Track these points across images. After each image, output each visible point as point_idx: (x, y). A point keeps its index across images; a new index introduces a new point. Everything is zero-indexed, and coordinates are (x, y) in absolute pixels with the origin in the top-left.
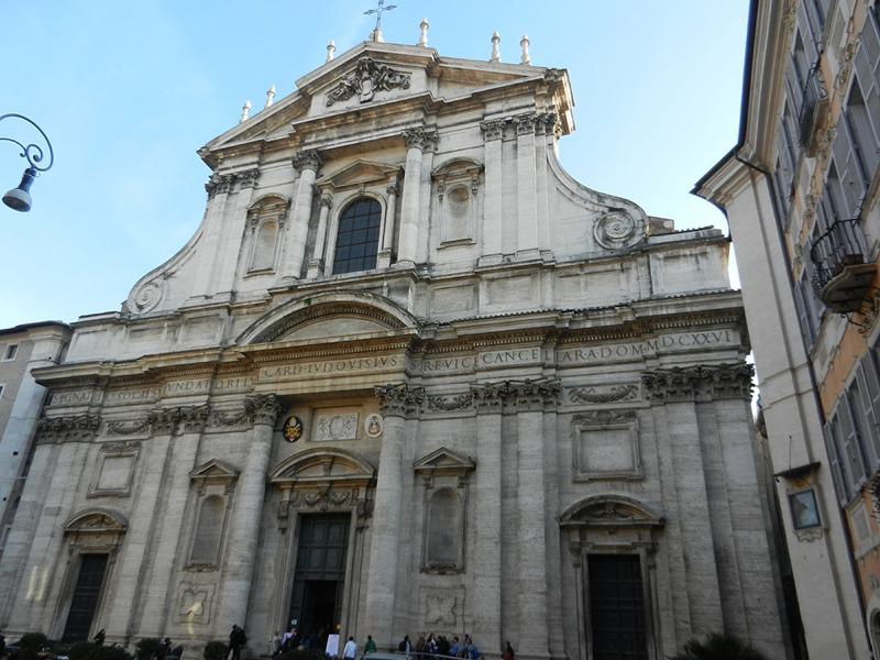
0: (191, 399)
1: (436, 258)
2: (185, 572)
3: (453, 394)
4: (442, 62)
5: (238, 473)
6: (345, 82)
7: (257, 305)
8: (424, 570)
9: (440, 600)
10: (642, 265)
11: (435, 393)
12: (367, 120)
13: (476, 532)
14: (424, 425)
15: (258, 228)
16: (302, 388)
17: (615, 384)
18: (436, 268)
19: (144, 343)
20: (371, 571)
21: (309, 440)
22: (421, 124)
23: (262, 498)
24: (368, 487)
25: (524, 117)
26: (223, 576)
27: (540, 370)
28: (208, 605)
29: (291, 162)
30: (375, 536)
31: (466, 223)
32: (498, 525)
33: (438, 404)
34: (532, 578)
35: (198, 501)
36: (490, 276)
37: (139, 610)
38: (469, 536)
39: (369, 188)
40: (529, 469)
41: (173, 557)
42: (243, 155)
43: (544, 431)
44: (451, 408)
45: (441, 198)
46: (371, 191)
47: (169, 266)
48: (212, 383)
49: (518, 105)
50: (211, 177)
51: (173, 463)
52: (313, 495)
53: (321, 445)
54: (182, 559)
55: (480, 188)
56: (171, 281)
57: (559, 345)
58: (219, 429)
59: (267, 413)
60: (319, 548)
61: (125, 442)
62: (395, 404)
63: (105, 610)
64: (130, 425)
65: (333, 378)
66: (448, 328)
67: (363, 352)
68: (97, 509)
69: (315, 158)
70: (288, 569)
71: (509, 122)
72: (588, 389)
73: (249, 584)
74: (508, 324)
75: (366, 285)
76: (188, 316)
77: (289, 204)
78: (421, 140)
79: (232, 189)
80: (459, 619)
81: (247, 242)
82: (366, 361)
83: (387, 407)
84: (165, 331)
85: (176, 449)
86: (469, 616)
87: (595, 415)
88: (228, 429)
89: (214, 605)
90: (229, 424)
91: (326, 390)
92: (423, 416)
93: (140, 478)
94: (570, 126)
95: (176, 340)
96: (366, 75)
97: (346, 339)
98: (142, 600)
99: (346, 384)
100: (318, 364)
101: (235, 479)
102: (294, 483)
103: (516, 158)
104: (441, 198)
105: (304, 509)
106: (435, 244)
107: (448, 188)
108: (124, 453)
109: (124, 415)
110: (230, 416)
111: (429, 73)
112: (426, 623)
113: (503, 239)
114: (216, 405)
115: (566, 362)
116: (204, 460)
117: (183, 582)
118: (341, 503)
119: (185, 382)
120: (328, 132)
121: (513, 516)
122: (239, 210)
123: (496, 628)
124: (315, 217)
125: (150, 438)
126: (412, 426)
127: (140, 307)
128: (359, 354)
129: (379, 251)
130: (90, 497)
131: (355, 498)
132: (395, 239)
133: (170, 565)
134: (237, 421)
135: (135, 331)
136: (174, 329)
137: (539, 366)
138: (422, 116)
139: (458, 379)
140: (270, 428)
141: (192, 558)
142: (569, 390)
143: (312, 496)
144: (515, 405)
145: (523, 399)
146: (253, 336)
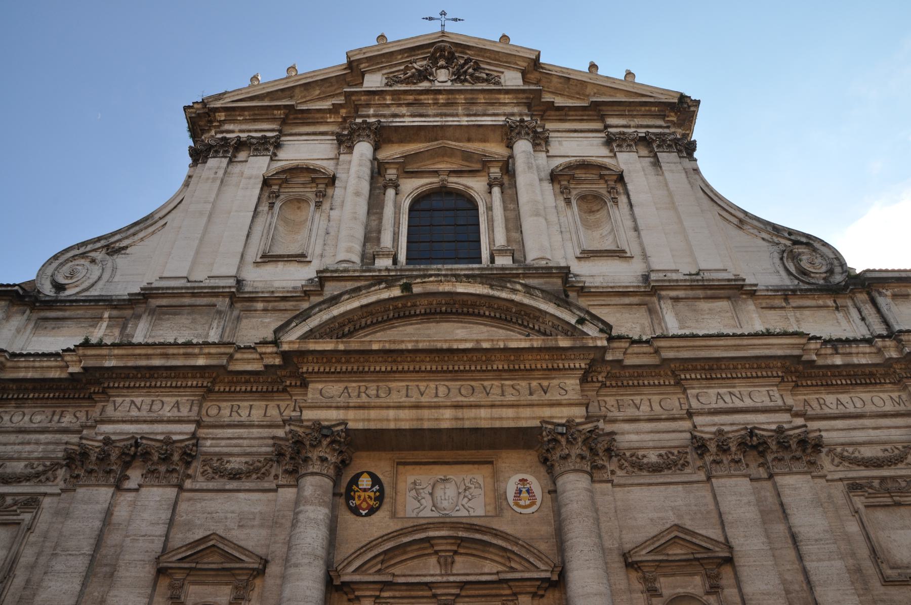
1: (577, 268)
3: (655, 448)
4: (543, 68)
5: (265, 562)
6: (415, 65)
7: (284, 299)
10: (864, 302)
11: (626, 445)
14: (620, 493)
15: (278, 204)
16: (396, 420)
17: (885, 443)
19: (62, 339)
21: (394, 515)
22: (529, 119)
27: (786, 417)
33: (638, 465)
36: (673, 294)
40: (820, 560)
42: (255, 120)
44: (656, 469)
48: (200, 407)
56: (120, 260)
58: (211, 485)
62: (579, 451)
65: (457, 406)
67: (509, 371)
71: (642, 139)
72: (851, 449)
74: (737, 347)
76: (154, 302)
77: (332, 180)
81: (261, 221)
82: (513, 386)
85: (121, 513)
87: (876, 483)
91: (445, 425)
96: (442, 63)
97: (485, 345)
99: (483, 418)
100: (422, 385)
101: (261, 572)
104: (568, 202)
107: (574, 192)
110: (235, 463)
113: (673, 256)
114: (209, 443)
115: (810, 412)
119: (148, 400)
126: (604, 494)
127: (59, 287)
128: (499, 374)
134: (248, 474)
135: (46, 319)
140: (328, 483)
144: (761, 465)
145: (779, 455)
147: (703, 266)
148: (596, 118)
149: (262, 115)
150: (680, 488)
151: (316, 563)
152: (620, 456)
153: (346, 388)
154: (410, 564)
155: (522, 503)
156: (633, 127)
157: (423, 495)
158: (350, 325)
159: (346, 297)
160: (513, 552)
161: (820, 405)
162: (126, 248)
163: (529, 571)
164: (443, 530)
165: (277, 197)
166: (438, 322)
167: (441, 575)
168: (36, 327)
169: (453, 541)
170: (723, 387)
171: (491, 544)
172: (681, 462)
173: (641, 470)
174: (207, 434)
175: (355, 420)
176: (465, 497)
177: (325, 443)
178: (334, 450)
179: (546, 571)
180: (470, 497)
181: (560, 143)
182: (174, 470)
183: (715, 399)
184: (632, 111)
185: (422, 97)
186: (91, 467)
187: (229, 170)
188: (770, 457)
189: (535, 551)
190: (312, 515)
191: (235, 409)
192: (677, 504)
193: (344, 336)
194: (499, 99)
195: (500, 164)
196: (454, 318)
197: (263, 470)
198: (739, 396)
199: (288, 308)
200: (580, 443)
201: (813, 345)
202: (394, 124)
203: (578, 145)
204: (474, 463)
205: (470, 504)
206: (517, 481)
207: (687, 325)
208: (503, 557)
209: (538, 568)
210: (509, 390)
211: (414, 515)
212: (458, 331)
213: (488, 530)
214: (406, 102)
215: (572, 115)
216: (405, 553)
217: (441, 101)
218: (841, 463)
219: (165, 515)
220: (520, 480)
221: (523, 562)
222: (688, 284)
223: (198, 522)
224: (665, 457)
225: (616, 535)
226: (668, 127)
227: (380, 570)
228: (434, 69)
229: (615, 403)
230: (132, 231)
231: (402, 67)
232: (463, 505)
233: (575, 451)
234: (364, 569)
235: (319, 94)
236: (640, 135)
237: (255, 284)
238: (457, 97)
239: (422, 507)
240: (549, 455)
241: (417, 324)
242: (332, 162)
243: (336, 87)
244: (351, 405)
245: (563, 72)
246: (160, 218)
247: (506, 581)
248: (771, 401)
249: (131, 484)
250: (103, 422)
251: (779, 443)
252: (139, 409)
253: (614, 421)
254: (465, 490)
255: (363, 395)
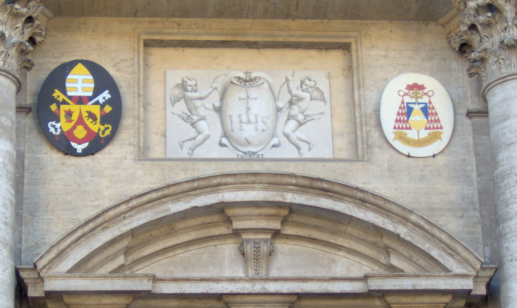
154: (182, 254)
155: (412, 134)
157: (202, 112)
160: (397, 237)
164: (253, 189)
167: (252, 280)
169: (273, 211)
171: (351, 220)
176: (290, 117)
178: (16, 16)
179: (464, 276)
180: (301, 117)
189: (443, 237)
205: (301, 133)
206: (403, 87)
208: (374, 245)
209: (447, 270)
211: (184, 154)
213: (346, 191)
216: (172, 232)
220: (410, 87)
221: (416, 257)
227: (121, 267)
232: (286, 135)
234: (90, 265)
239: (200, 138)
240: (475, 39)
247: (383, 294)
254: (291, 103)
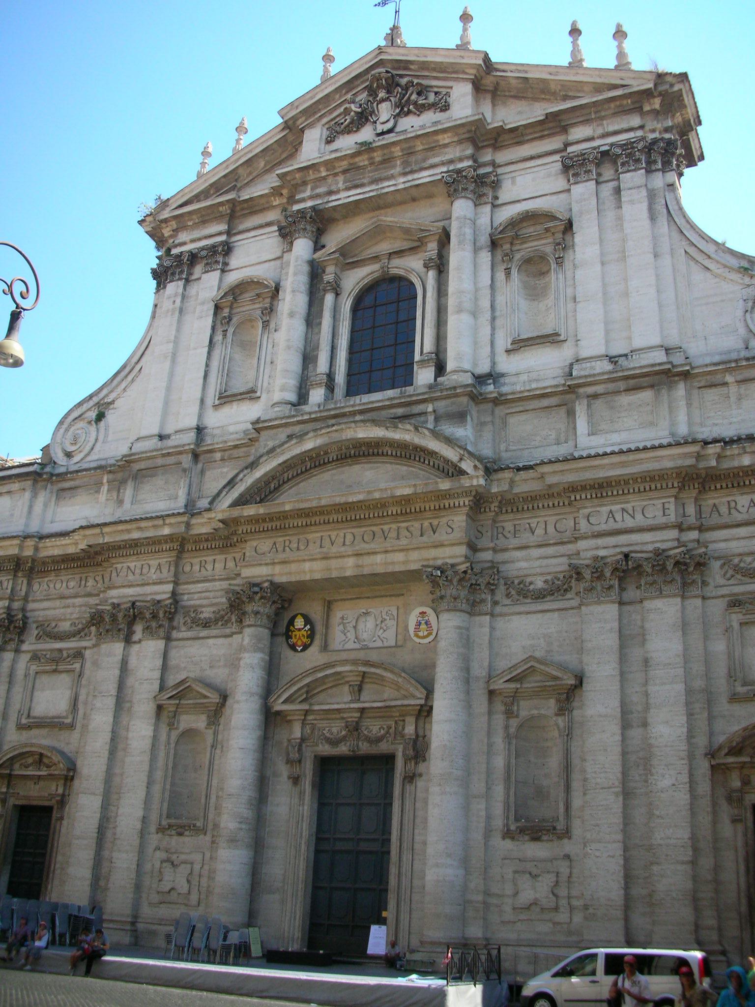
0: (148, 589)
1: (506, 364)
2: (160, 835)
4: (497, 70)
6: (353, 107)
7: (236, 447)
8: (508, 834)
9: (534, 877)
11: (515, 573)
12: (387, 161)
13: (585, 780)
14: (500, 623)
15: (231, 330)
18: (507, 380)
19: (77, 507)
20: (432, 838)
21: (325, 648)
23: (259, 733)
24: (418, 716)
25: (628, 146)
26: (213, 842)
27: (674, 534)
28: (195, 882)
29: (275, 228)
30: (434, 789)
31: (547, 310)
32: (618, 769)
34: (672, 841)
35: (169, 736)
36: (590, 390)
37: (102, 883)
38: (576, 785)
39: (396, 262)
40: (663, 684)
41: (140, 813)
43: (684, 626)
44: (540, 596)
45: (508, 272)
46: (398, 267)
47: (105, 392)
48: (177, 566)
49: (616, 127)
50: (158, 257)
51: (130, 681)
52: (336, 728)
53: (344, 656)
54: (154, 817)
55: (569, 256)
56: (111, 417)
57: (703, 490)
58: (189, 634)
59: (261, 610)
60: (349, 804)
61: (60, 650)
62: (454, 592)
63: (56, 882)
64: (65, 626)
66: (531, 473)
68: (32, 745)
69: (313, 220)
70: (305, 833)
72: (749, 559)
73: (252, 853)
74: (623, 464)
75: (400, 411)
78: (472, 187)
79: (190, 274)
80: (563, 902)
81: (216, 353)
83: (442, 597)
84: (105, 488)
85: (133, 662)
86: (577, 898)
88: (204, 633)
89: (204, 881)
90: (205, 626)
92: (498, 609)
93: (86, 703)
94: (696, 154)
95: (120, 502)
96: (382, 94)
98: (104, 871)
99: (377, 563)
100: (333, 534)
102: (307, 712)
103: (620, 207)
104: (508, 272)
105: (325, 749)
106: (503, 342)
107: (518, 256)
108: (61, 668)
109: (57, 612)
111: (478, 87)
112: (514, 909)
114: (186, 597)
116: (172, 680)
117: (158, 848)
118: (379, 740)
119: (139, 564)
120: (330, 180)
121: (641, 754)
122: (203, 303)
123: (620, 914)
124: (314, 309)
125: (94, 646)
127: (69, 455)
129: (417, 357)
130: (20, 727)
131: (399, 734)
132: (440, 338)
133: (139, 826)
135: (63, 490)
136: (118, 486)
137: (674, 527)
138: (469, 151)
139: (550, 550)
140: (266, 633)
141: (168, 817)
142: (719, 563)
143: (335, 730)
146: (235, 494)
147: (638, 343)
148: (558, 130)
149: (208, 215)
150: (556, 614)
151: (252, 699)
152: (509, 583)
153: (275, 543)
155: (421, 634)
156: (598, 138)
158: (275, 481)
159: (264, 458)
161: (729, 509)
162: (113, 402)
163: (405, 697)
165: (228, 322)
166: (351, 465)
168: (58, 498)
170: (616, 504)
172: (565, 587)
173: (525, 597)
174: (184, 590)
175: (281, 574)
177: (257, 597)
181: (514, 183)
182: (160, 626)
183: (605, 518)
184: (600, 111)
185: (357, 160)
186: (107, 627)
187: (186, 293)
188: (643, 582)
190: (248, 661)
191: (203, 563)
192: (549, 631)
193: (270, 492)
194: (438, 141)
195: (437, 237)
196: (363, 460)
197: (226, 618)
198: (631, 512)
199: (241, 455)
200: (455, 583)
201: (713, 449)
202: (331, 205)
203: (534, 180)
204: (391, 596)
207: (600, 428)
210: (404, 532)
211: (340, 648)
212: (368, 473)
214: (341, 169)
215: (531, 134)
216: (324, 683)
217: (378, 159)
218: (732, 576)
219: (159, 663)
222: (606, 377)
223: (183, 665)
224: (550, 583)
225: (486, 664)
226: (642, 127)
228: (375, 104)
229: (512, 529)
230: (115, 382)
231: (342, 109)
233: (451, 591)
235: (265, 165)
236: (603, 149)
237: (216, 432)
238: (393, 150)
241: (333, 469)
242: (278, 262)
243: (280, 151)
244: (276, 561)
245: (519, 71)
246: (137, 363)
247: (395, 706)
248: (664, 515)
249: (137, 637)
250: (109, 588)
251: (653, 566)
252: (134, 574)
253: (505, 550)
255: (287, 549)
